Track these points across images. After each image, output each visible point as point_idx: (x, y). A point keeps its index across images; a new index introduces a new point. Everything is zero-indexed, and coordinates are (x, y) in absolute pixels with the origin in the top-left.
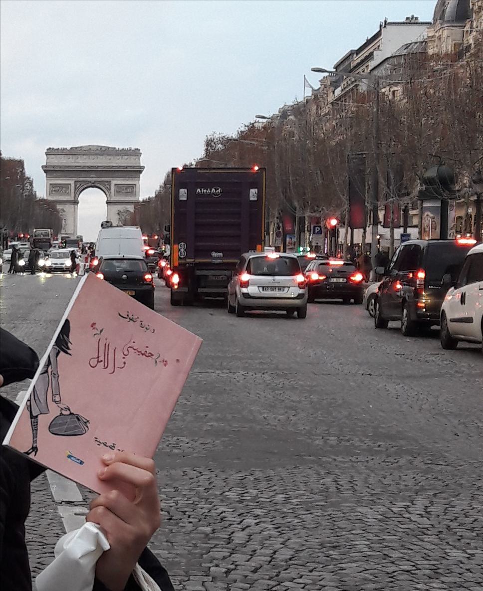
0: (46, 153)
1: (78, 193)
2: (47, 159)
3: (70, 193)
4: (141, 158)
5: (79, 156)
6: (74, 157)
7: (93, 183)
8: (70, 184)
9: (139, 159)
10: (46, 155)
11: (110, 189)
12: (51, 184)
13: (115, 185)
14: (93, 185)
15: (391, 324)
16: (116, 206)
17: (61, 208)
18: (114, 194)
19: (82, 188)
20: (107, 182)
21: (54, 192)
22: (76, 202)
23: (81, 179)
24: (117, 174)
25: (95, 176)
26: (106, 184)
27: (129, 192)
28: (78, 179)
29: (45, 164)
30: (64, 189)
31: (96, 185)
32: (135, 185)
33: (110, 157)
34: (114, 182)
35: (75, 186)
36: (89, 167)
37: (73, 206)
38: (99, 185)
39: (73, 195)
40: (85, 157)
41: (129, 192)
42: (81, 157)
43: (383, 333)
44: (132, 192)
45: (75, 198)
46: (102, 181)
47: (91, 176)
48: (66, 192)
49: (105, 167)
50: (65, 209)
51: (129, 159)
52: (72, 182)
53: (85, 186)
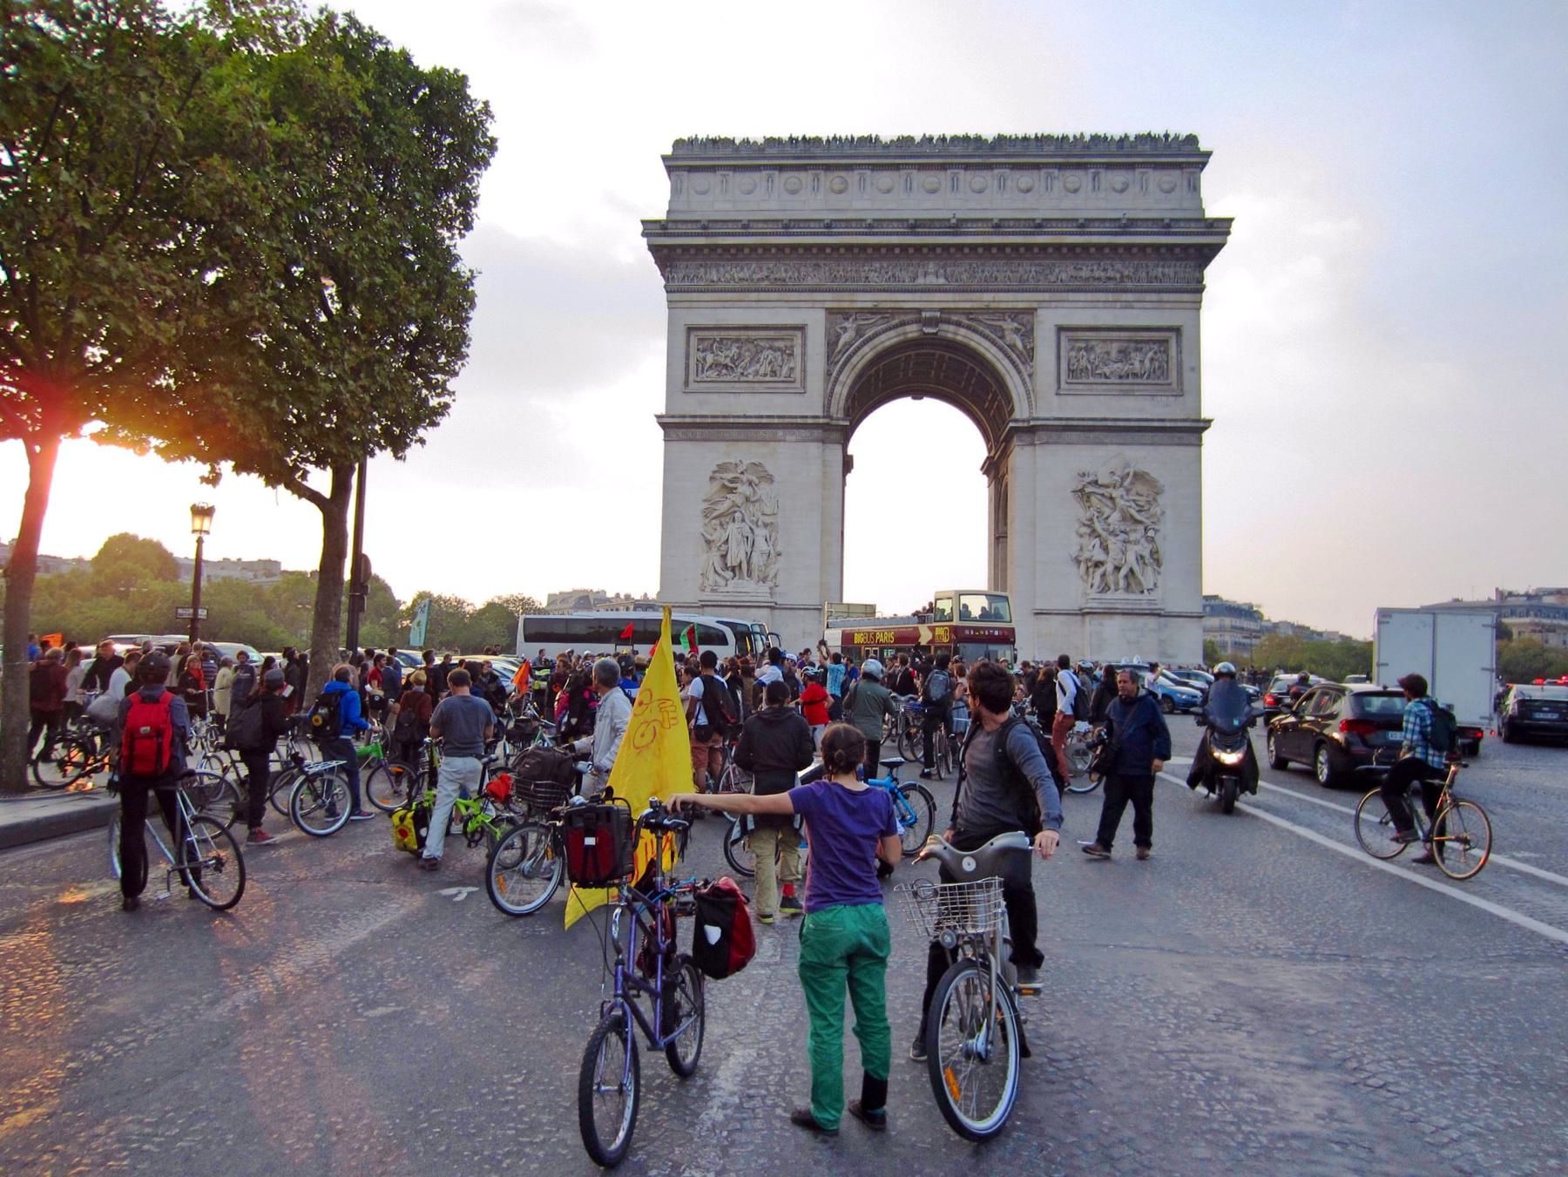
0: (664, 158)
1: (847, 379)
2: (675, 191)
3: (797, 374)
4: (1207, 177)
5: (853, 177)
6: (827, 179)
7: (933, 322)
8: (801, 328)
9: (1195, 188)
10: (670, 169)
11: (1029, 355)
12: (691, 329)
13: (1061, 329)
14: (928, 330)
15: (1292, 765)
16: (1062, 450)
17: (747, 462)
18: (1052, 380)
19: (868, 353)
20: (1015, 314)
21: (713, 374)
22: (837, 430)
23: (865, 300)
24: (1064, 271)
25: (942, 281)
26: (1009, 325)
27: (1135, 375)
28: (845, 300)
29: (660, 214)
30: (766, 353)
31: (949, 331)
32: (1177, 330)
33: (1025, 179)
34: (1048, 320)
35: (831, 344)
36: (915, 226)
37: (814, 449)
38: (962, 335)
39: (816, 383)
40: (885, 178)
41: (1135, 375)
42: (862, 180)
43: (1280, 775)
44: (1160, 371)
45: (827, 406)
46: (987, 310)
47: (920, 281)
48: (774, 373)
49: (999, 226)
50: (770, 469)
51: (1134, 189)
52: (816, 321)
53: (889, 339)
